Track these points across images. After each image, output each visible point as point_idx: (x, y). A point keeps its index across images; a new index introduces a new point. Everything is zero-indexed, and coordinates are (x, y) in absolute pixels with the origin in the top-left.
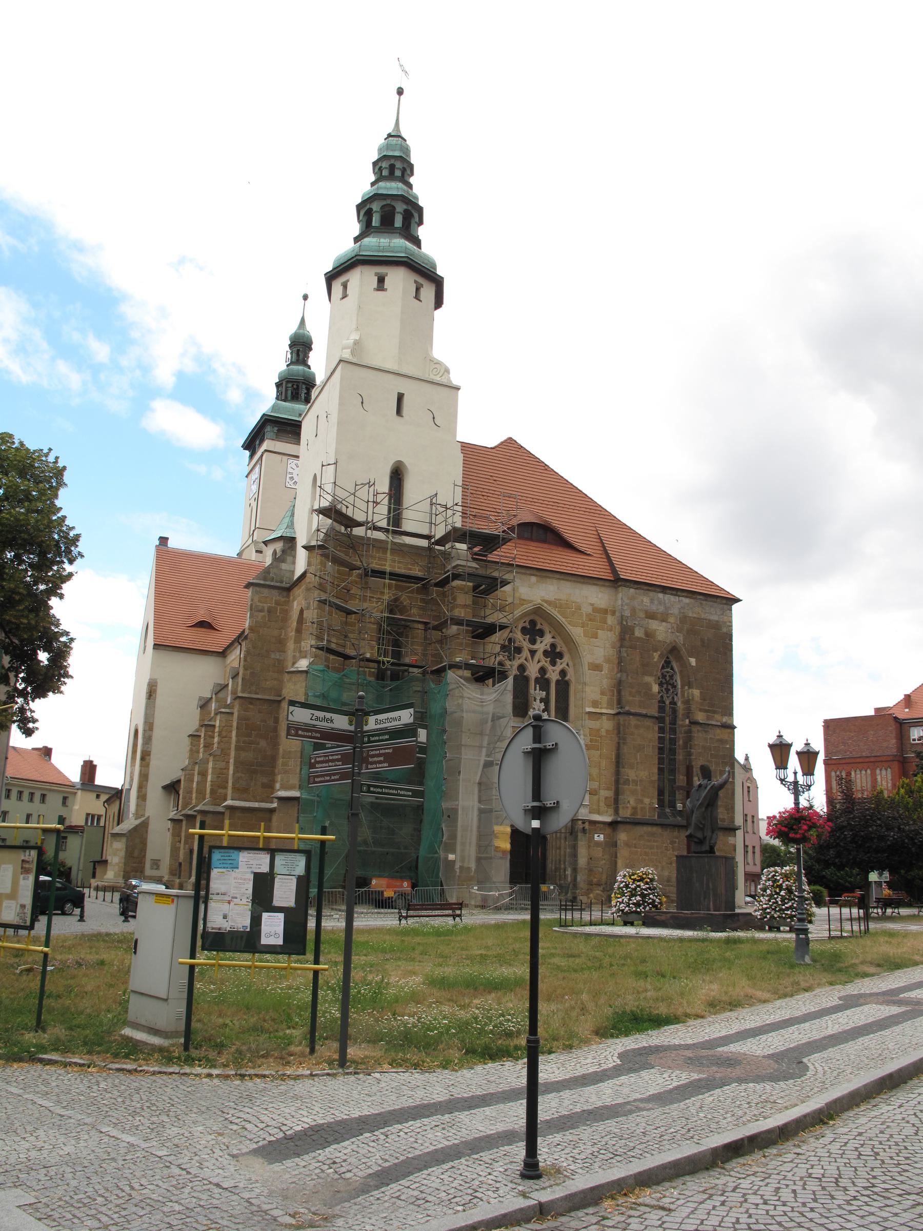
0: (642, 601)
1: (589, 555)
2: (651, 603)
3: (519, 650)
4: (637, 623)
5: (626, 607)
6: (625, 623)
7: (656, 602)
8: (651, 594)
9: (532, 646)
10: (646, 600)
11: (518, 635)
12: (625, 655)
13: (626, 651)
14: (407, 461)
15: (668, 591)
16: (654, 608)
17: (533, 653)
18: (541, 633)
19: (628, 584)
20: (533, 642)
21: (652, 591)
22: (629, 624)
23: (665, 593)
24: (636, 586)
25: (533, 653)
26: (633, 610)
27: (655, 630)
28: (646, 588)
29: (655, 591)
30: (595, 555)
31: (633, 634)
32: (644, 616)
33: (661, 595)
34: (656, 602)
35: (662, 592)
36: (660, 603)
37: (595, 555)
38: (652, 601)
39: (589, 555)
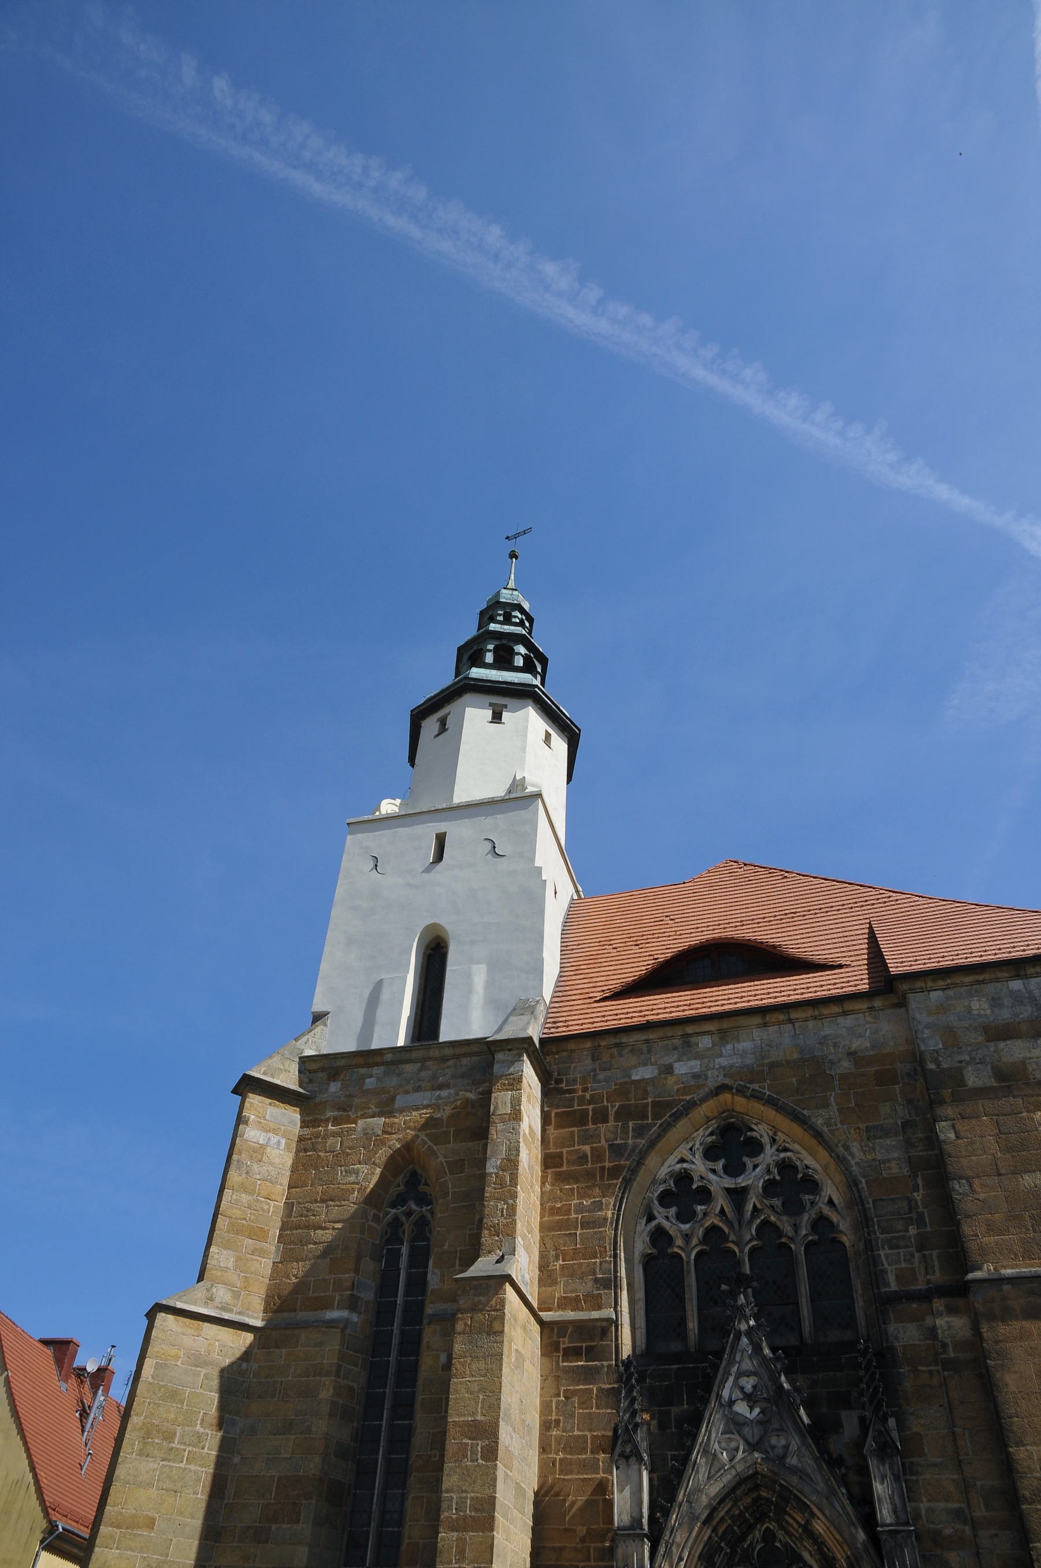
0: (969, 1010)
1: (840, 966)
2: (992, 1007)
3: (705, 1194)
4: (967, 1058)
5: (927, 1033)
6: (932, 1066)
7: (1007, 1002)
8: (990, 988)
9: (729, 1182)
10: (979, 1006)
11: (699, 1166)
12: (952, 1136)
13: (953, 1127)
14: (447, 922)
15: (1030, 971)
16: (1005, 1014)
17: (737, 1195)
18: (755, 1147)
19: (919, 984)
20: (734, 1169)
21: (991, 981)
22: (945, 1066)
23: (1026, 977)
24: (941, 983)
25: (737, 1195)
26: (950, 1034)
27: (1023, 1062)
28: (969, 979)
29: (997, 980)
30: (855, 964)
31: (962, 1082)
32: (981, 1039)
33: (1016, 985)
34: (1007, 1002)
35: (1017, 976)
36: (1017, 998)
37: (855, 964)
38: (995, 1002)
39: (840, 966)
